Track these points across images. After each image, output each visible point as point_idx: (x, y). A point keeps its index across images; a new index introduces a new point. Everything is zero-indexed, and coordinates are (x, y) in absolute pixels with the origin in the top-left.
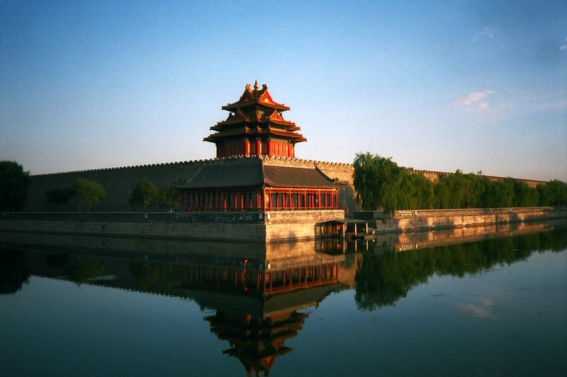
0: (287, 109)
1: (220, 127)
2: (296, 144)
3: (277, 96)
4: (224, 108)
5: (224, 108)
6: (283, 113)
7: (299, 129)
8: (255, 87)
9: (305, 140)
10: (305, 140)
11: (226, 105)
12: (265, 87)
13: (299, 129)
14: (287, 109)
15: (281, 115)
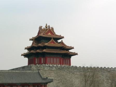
0: (63, 38)
1: (29, 49)
2: (72, 57)
3: (58, 32)
4: (30, 40)
5: (30, 40)
6: (62, 39)
7: (73, 48)
8: (46, 27)
9: (77, 54)
10: (77, 54)
11: (31, 38)
12: (49, 26)
13: (73, 48)
14: (63, 38)
15: (62, 41)
